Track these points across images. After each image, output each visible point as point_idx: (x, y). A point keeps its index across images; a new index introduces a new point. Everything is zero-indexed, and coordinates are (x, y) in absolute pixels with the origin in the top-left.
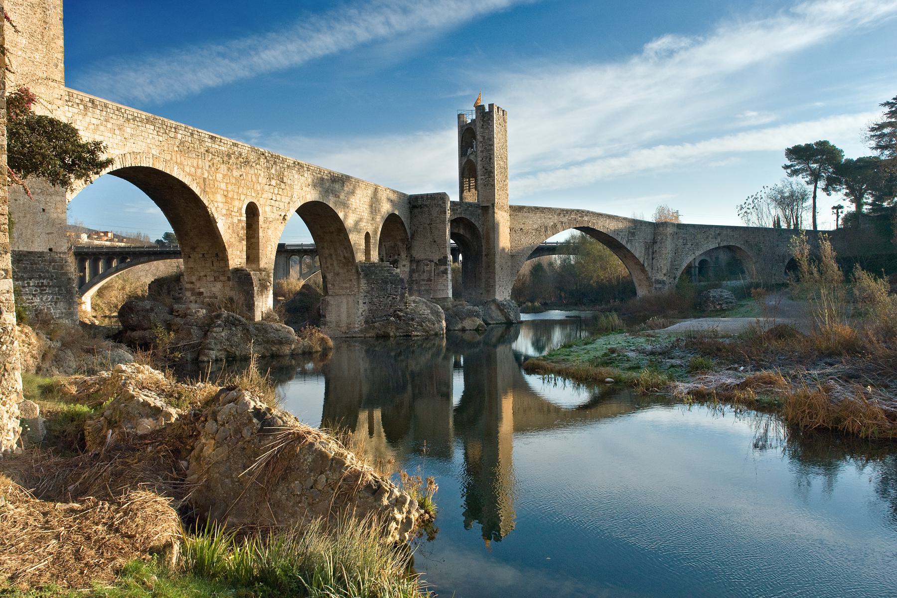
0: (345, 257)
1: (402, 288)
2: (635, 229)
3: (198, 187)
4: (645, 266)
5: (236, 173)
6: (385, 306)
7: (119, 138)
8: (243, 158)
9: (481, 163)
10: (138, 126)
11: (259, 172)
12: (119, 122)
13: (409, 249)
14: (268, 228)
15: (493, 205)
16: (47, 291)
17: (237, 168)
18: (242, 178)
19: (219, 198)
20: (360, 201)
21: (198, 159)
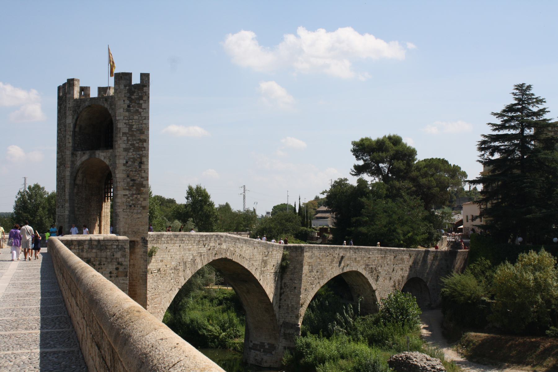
9: (124, 168)
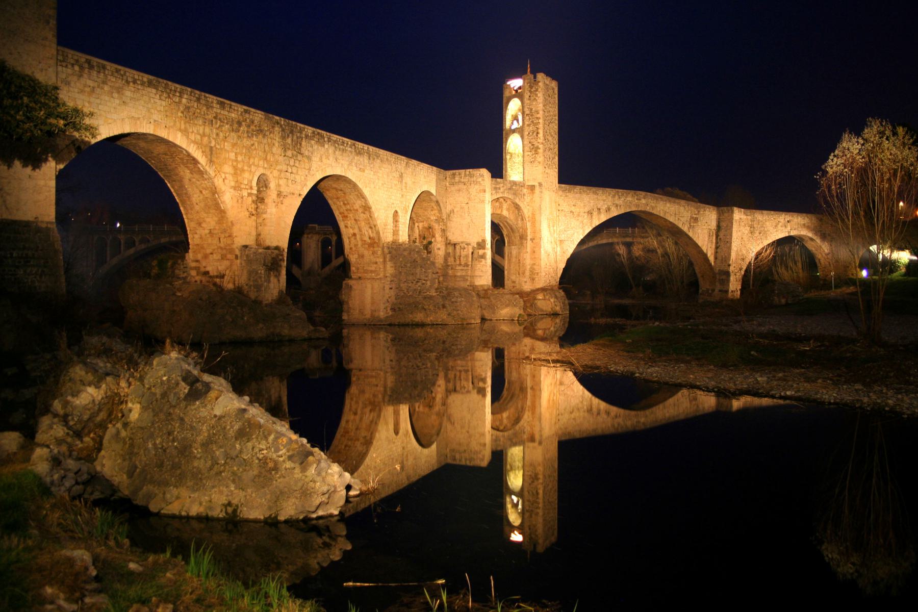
0: (370, 238)
1: (433, 273)
2: (698, 214)
3: (204, 157)
4: (709, 255)
5: (247, 142)
6: (413, 292)
7: (117, 101)
8: (256, 126)
10: (138, 89)
11: (275, 142)
12: (117, 85)
13: (443, 231)
14: (282, 204)
15: (540, 184)
16: (32, 263)
17: (248, 136)
18: (253, 148)
19: (228, 169)
20: (388, 176)
21: (204, 125)
